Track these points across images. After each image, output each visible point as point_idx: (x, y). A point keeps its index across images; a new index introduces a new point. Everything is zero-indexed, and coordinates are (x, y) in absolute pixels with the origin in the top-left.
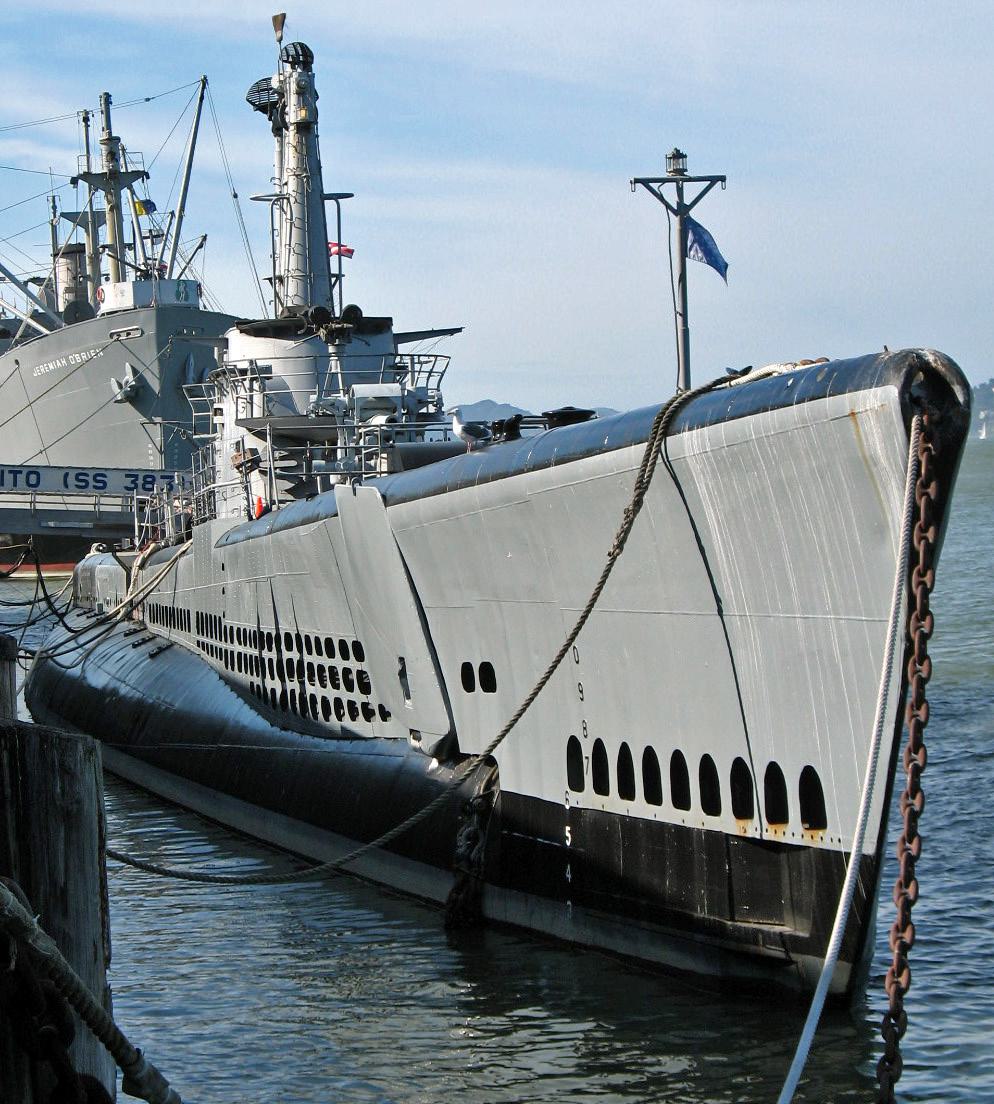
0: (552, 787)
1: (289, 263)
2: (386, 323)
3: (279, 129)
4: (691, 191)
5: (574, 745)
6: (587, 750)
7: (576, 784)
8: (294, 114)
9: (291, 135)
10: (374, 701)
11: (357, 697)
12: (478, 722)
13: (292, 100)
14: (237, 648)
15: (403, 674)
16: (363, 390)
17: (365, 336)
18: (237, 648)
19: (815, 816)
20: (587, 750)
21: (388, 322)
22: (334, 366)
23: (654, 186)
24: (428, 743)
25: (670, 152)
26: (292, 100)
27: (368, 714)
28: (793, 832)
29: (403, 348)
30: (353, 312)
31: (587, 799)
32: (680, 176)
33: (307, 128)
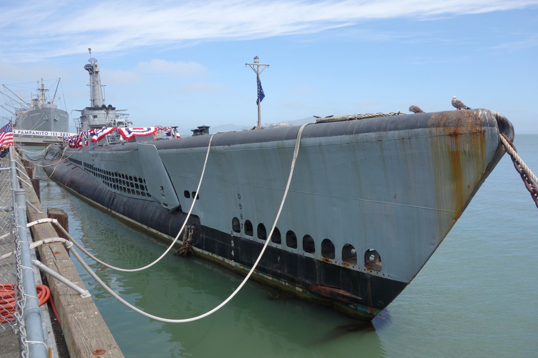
0: (226, 228)
2: (114, 109)
3: (90, 74)
4: (261, 68)
5: (235, 220)
6: (242, 222)
10: (145, 191)
11: (140, 190)
14: (98, 172)
20: (242, 222)
23: (252, 66)
25: (255, 57)
27: (143, 194)
29: (117, 113)
30: (110, 106)
31: (243, 235)
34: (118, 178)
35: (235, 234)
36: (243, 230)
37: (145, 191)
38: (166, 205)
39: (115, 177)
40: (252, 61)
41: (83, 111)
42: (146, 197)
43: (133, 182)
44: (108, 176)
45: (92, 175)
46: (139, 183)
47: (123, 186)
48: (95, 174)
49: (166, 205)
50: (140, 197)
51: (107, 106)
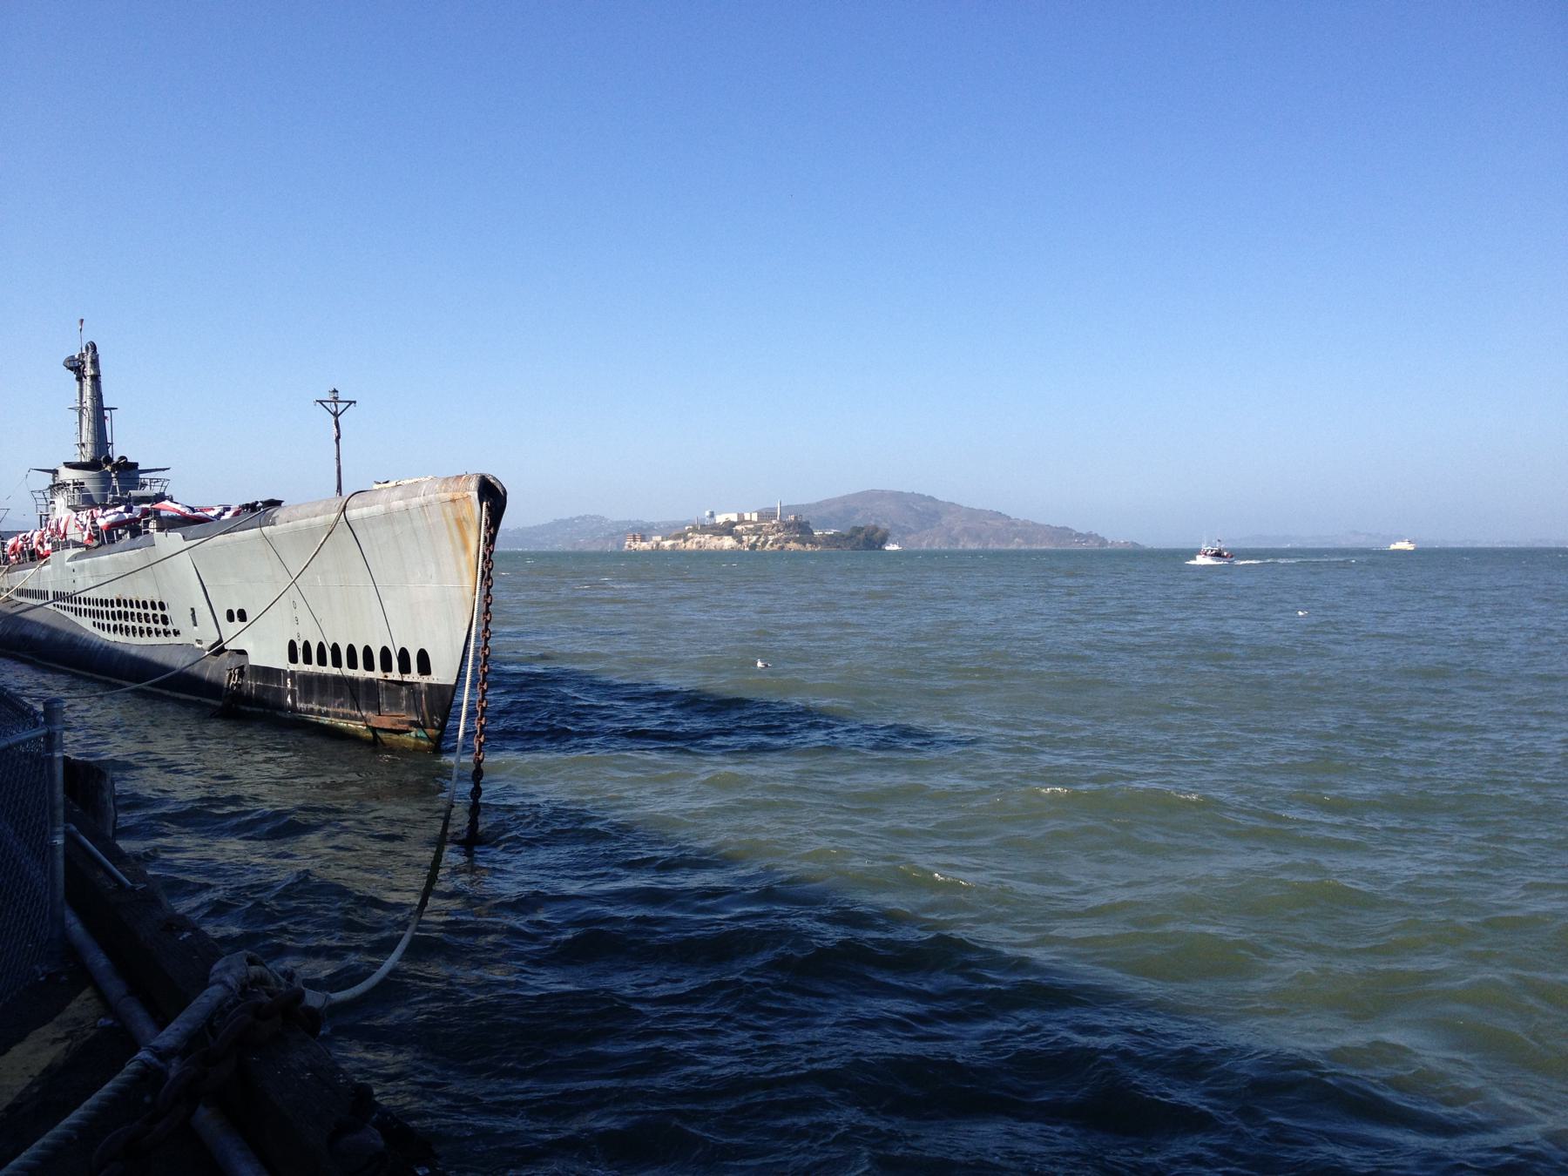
0: (281, 662)
1: (87, 437)
2: (136, 465)
3: (80, 379)
4: (341, 406)
5: (292, 645)
6: (300, 645)
7: (293, 659)
8: (89, 371)
9: (88, 382)
10: (170, 627)
11: (161, 626)
12: (237, 637)
13: (88, 365)
14: (83, 606)
15: (193, 615)
16: (133, 493)
17: (128, 470)
18: (83, 606)
19: (425, 667)
20: (300, 645)
21: (136, 465)
22: (115, 483)
24: (206, 645)
26: (88, 365)
27: (166, 633)
28: (414, 676)
31: (300, 667)
32: (336, 400)
33: (96, 379)
34: (122, 609)
35: (293, 667)
36: (300, 658)
37: (170, 627)
38: (199, 642)
39: (116, 609)
40: (328, 397)
41: (55, 472)
42: (172, 639)
43: (150, 611)
44: (104, 609)
45: (71, 615)
46: (159, 612)
47: (130, 624)
48: (78, 612)
49: (199, 642)
50: (162, 640)
51: (116, 460)
